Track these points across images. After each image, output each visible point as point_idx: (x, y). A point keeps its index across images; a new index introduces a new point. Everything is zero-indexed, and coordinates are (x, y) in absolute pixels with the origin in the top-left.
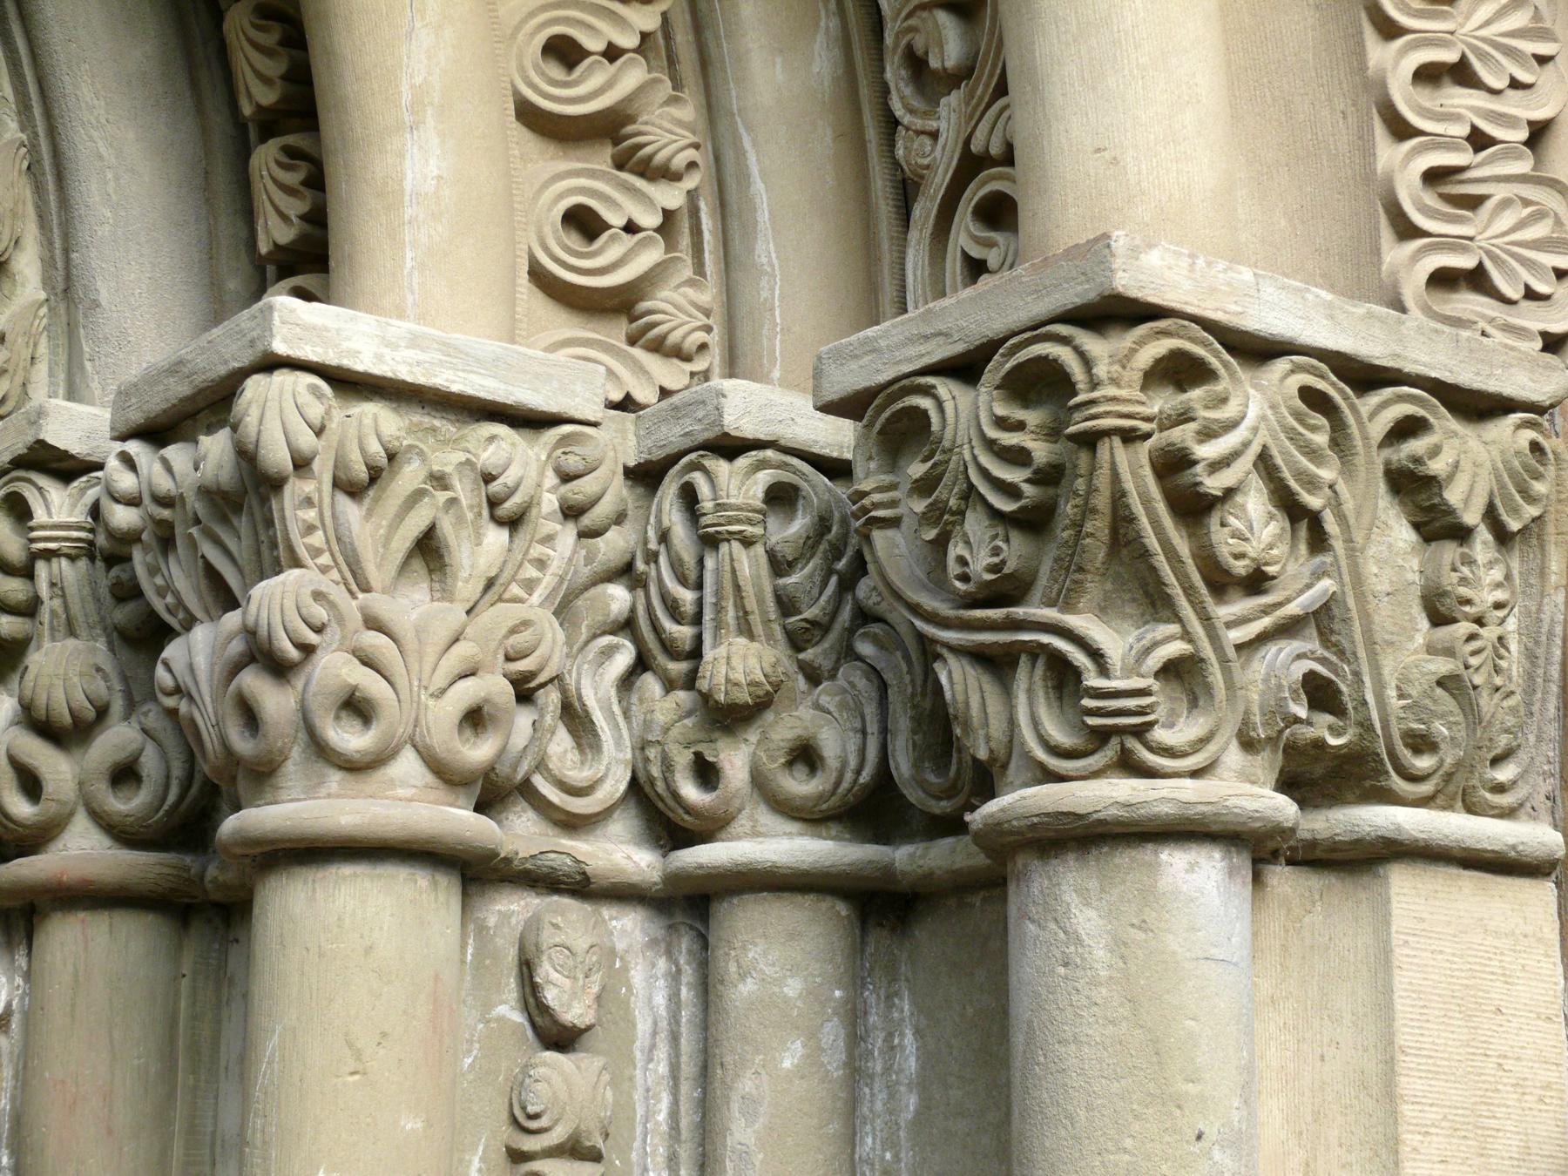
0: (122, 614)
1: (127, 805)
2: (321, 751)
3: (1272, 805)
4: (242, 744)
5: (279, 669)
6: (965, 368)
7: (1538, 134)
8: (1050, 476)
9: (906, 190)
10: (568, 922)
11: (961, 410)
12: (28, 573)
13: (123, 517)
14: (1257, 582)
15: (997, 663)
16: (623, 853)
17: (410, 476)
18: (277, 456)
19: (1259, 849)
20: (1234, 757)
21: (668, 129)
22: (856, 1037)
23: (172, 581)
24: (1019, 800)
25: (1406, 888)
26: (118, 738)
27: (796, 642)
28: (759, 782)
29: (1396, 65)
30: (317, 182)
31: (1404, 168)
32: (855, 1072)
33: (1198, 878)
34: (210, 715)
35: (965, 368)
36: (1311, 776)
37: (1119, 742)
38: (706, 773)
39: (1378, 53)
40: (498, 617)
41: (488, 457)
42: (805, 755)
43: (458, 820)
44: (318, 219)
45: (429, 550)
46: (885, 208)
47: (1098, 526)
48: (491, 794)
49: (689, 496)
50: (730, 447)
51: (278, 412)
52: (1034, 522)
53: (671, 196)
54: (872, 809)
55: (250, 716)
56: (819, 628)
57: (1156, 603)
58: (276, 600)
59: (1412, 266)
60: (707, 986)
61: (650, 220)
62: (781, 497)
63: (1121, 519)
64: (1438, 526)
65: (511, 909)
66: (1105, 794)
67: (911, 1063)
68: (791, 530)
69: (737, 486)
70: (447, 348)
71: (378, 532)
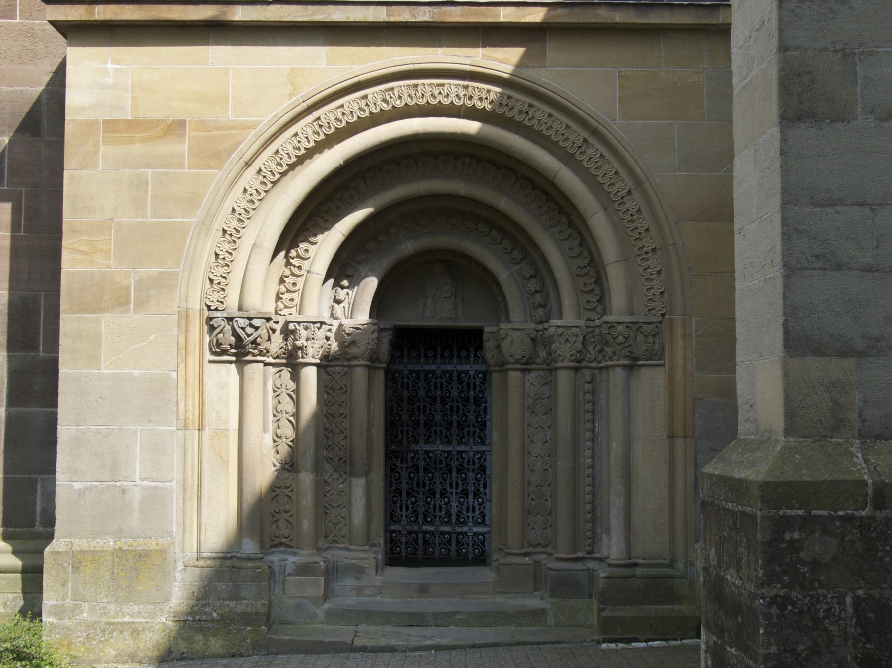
3: (627, 362)
45: (567, 340)
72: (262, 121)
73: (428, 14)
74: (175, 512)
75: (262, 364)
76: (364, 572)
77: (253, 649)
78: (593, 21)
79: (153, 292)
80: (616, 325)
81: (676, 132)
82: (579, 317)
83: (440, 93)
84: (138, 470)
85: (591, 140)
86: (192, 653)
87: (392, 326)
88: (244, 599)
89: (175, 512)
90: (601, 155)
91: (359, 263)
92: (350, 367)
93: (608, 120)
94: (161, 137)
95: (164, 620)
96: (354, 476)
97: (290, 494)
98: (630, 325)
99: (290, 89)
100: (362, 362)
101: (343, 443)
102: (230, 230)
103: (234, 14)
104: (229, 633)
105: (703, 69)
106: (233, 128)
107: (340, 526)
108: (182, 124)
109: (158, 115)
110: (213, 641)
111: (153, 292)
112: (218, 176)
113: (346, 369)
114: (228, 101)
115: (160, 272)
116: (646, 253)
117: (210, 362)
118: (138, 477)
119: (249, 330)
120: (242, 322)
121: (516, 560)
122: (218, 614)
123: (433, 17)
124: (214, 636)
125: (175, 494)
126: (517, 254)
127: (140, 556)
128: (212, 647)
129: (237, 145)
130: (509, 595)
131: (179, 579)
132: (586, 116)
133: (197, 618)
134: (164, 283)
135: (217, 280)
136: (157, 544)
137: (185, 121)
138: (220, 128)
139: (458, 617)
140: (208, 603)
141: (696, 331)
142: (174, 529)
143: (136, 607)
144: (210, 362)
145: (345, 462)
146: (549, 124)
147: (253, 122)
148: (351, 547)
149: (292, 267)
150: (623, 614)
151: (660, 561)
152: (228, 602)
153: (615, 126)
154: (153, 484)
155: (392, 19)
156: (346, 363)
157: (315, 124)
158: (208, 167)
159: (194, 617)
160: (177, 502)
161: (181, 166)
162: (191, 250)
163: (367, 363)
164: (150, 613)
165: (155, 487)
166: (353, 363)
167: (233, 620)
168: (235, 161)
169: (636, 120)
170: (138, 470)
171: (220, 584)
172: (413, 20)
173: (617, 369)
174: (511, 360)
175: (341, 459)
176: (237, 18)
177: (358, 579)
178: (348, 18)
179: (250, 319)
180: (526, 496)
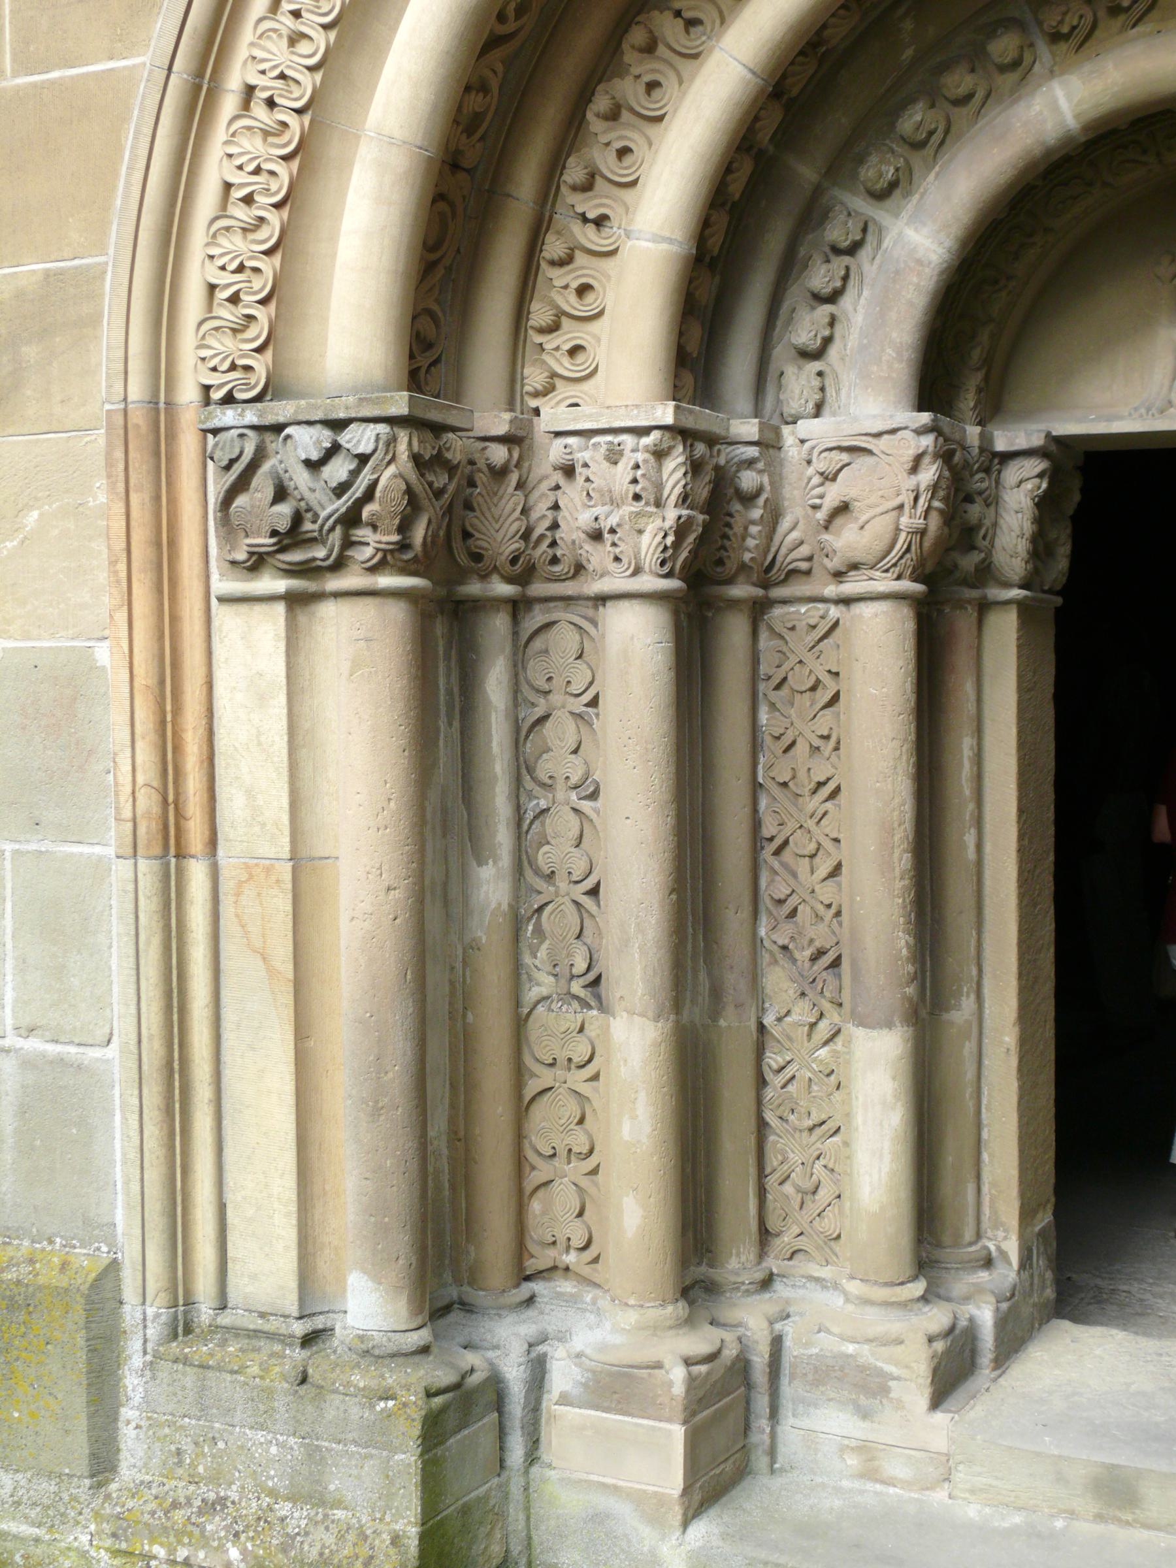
74: (118, 1156)
76: (884, 1390)
79: (30, 352)
87: (1037, 441)
88: (338, 1504)
89: (118, 1156)
91: (881, 195)
92: (846, 601)
95: (85, 1539)
100: (885, 584)
101: (827, 892)
102: (266, 84)
107: (824, 1195)
111: (30, 352)
113: (834, 612)
115: (47, 274)
117: (222, 600)
122: (244, 1552)
125: (117, 1092)
131: (137, 1398)
133: (182, 1554)
136: (64, 1266)
140: (222, 1501)
142: (119, 1216)
145: (836, 963)
149: (576, 228)
159: (172, 1551)
160: (124, 1119)
163: (907, 585)
165: (61, 1062)
171: (260, 1436)
175: (821, 953)
177: (865, 1415)
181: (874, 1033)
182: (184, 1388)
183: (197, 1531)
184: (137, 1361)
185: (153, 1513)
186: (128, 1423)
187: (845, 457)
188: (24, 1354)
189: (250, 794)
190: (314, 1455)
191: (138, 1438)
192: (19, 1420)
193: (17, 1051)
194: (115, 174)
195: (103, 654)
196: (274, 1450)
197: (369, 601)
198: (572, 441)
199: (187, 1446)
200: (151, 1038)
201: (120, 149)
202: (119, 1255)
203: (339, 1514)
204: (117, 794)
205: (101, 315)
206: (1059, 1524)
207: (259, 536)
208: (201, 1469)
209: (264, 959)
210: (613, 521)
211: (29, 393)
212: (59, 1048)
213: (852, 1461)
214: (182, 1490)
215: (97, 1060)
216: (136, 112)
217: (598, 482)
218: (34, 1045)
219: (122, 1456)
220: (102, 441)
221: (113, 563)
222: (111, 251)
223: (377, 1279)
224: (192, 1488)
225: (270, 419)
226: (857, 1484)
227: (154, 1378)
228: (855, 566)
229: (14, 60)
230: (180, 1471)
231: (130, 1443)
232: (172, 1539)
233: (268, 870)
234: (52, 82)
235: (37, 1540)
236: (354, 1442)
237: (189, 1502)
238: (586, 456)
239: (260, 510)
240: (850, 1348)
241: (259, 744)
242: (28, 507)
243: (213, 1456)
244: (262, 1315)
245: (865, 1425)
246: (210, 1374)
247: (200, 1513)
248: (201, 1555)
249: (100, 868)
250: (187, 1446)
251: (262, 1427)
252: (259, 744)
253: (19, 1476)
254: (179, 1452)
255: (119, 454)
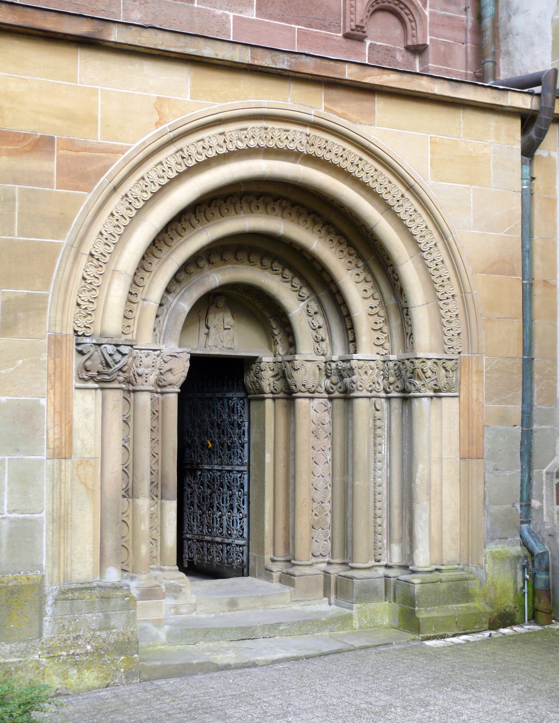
0: (339, 374)
1: (340, 390)
2: (358, 390)
3: (432, 394)
4: (352, 389)
5: (354, 383)
6: (408, 359)
7: (459, 334)
8: (413, 370)
9: (407, 334)
10: (378, 401)
11: (407, 362)
12: (331, 370)
13: (340, 368)
14: (430, 377)
15: (410, 383)
16: (383, 394)
17: (364, 367)
18: (354, 367)
19: (431, 397)
20: (428, 390)
21: (385, 329)
22: (402, 409)
23: (344, 374)
24: (412, 394)
25: (443, 399)
26: (340, 384)
27: (397, 377)
28: (393, 389)
29: (445, 330)
30: (354, 334)
31: (446, 339)
32: (402, 413)
33: (425, 400)
34: (349, 386)
35: (408, 359)
36: (435, 391)
37: (419, 390)
38: (389, 388)
39: (444, 328)
40: (372, 377)
41: (370, 364)
42: (397, 387)
43: (369, 394)
44: (355, 338)
45: (366, 372)
46: (405, 334)
47: (416, 375)
48: (371, 391)
49: (387, 365)
50: (391, 361)
51: (354, 363)
52: (412, 373)
53: (386, 335)
54: (404, 391)
55: (352, 387)
56: (399, 376)
57: (421, 380)
58: (354, 378)
59: (446, 347)
60: (390, 405)
61: (384, 338)
62: (395, 365)
63: (418, 375)
64: (446, 370)
65: (373, 399)
66: (418, 394)
67: (407, 412)
68: (396, 367)
69: (391, 364)
70: (367, 356)
71: (362, 372)
72: (130, 147)
73: (286, 63)
75: (122, 391)
76: (181, 591)
77: (126, 677)
78: (417, 89)
79: (21, 315)
80: (425, 360)
81: (472, 195)
82: (372, 353)
83: (287, 138)
84: (6, 502)
85: (407, 195)
86: (66, 689)
88: (114, 628)
90: (415, 211)
92: (162, 393)
93: (422, 179)
94: (29, 151)
95: (37, 657)
96: (168, 499)
97: (125, 519)
98: (436, 361)
99: (156, 117)
102: (97, 255)
103: (110, 34)
104: (103, 664)
105: (491, 143)
106: (102, 151)
108: (51, 140)
109: (23, 128)
110: (86, 673)
111: (21, 315)
112: (89, 198)
114: (97, 122)
115: (28, 294)
116: (448, 298)
117: (76, 388)
118: (6, 509)
119: (118, 357)
120: (111, 349)
121: (307, 570)
122: (92, 646)
123: (290, 66)
124: (88, 668)
126: (305, 291)
127: (12, 593)
128: (86, 680)
129: (106, 168)
130: (302, 603)
132: (406, 174)
133: (71, 652)
134: (33, 306)
135: (84, 305)
136: (28, 579)
137: (53, 138)
138: (90, 150)
139: (281, 628)
140: (79, 636)
141: (486, 368)
142: (44, 562)
143: (8, 647)
144: (76, 388)
146: (375, 177)
147: (121, 146)
148: (166, 567)
150: (435, 614)
151: (456, 566)
152: (98, 633)
153: (427, 185)
154: (21, 516)
155: (256, 63)
156: (159, 390)
157: (178, 154)
158: (77, 188)
159: (68, 652)
160: (47, 533)
161: (49, 184)
162: (61, 272)
164: (22, 651)
165: (24, 519)
166: (164, 390)
167: (107, 651)
168: (104, 182)
169: (443, 181)
170: (6, 502)
171: (90, 615)
172: (274, 66)
173: (423, 399)
174: (303, 389)
176: (112, 39)
177: (176, 598)
178: (217, 55)
179: (117, 345)
180: (311, 511)
181: (172, 502)
182: (66, 607)
183: (76, 645)
184: (50, 603)
185: (60, 644)
186: (46, 621)
187: (170, 357)
188: (16, 607)
189: (83, 441)
190: (107, 617)
191: (50, 625)
192: (13, 627)
193: (8, 518)
194: (52, 269)
195: (43, 402)
196: (94, 618)
197: (119, 390)
198: (137, 351)
199: (66, 623)
200: (57, 509)
201: (54, 264)
202: (44, 573)
203: (114, 631)
204: (48, 441)
205: (47, 308)
206: (222, 614)
207: (94, 372)
208: (71, 629)
209: (85, 485)
210: (147, 372)
211: (20, 326)
212: (23, 515)
213: (172, 611)
214: (66, 636)
215: (38, 517)
216: (60, 255)
217: (144, 362)
218: (15, 515)
219: (44, 632)
220: (47, 343)
221: (49, 377)
222: (51, 290)
223: (117, 568)
224: (68, 635)
225: (100, 342)
226: (174, 616)
227: (56, 606)
228: (170, 385)
229: (18, 232)
230: (64, 631)
231: (47, 627)
232: (68, 649)
233: (87, 461)
234: (32, 241)
235: (20, 662)
236: (119, 610)
237: (69, 639)
238: (140, 355)
239: (96, 365)
240: (172, 582)
241: (86, 427)
242: (19, 359)
243: (75, 624)
244: (82, 584)
245: (176, 601)
246: (74, 601)
247: (74, 640)
248: (78, 650)
249: (41, 462)
250: (66, 623)
251: (91, 612)
252: (86, 427)
253: (12, 645)
254: (63, 626)
255: (52, 347)
